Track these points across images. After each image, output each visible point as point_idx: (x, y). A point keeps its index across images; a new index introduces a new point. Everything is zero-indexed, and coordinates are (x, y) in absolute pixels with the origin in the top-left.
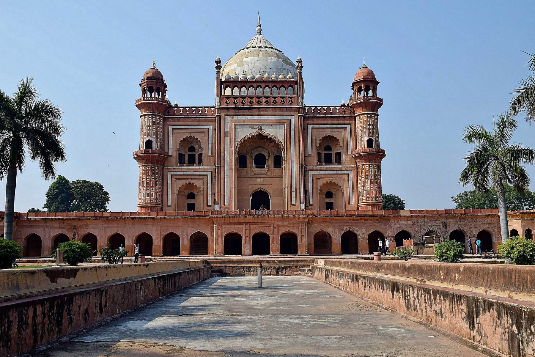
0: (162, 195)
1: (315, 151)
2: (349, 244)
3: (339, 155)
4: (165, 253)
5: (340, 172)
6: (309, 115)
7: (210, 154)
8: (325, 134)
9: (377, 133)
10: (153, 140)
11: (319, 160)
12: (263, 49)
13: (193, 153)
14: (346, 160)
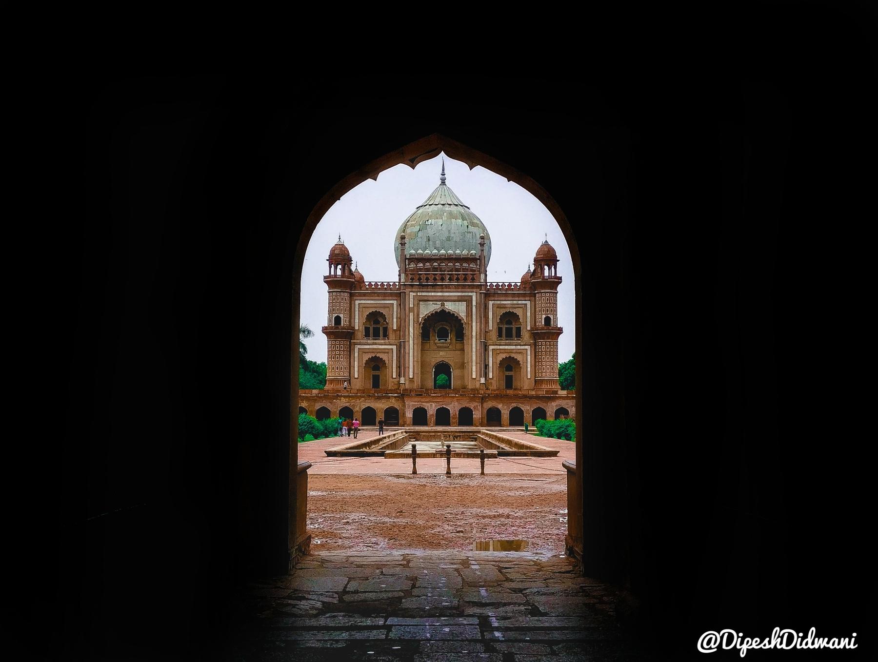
0: (350, 367)
1: (496, 326)
2: (516, 419)
3: (519, 330)
4: (363, 424)
5: (519, 347)
6: (492, 292)
7: (395, 328)
8: (504, 311)
9: (556, 311)
10: (342, 316)
11: (500, 335)
12: (447, 208)
13: (378, 326)
14: (526, 335)
